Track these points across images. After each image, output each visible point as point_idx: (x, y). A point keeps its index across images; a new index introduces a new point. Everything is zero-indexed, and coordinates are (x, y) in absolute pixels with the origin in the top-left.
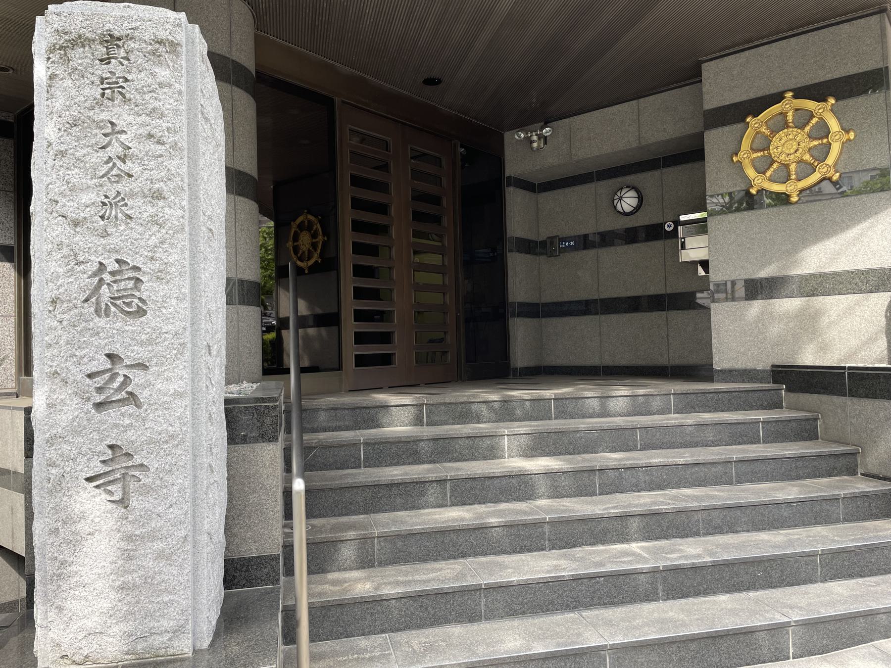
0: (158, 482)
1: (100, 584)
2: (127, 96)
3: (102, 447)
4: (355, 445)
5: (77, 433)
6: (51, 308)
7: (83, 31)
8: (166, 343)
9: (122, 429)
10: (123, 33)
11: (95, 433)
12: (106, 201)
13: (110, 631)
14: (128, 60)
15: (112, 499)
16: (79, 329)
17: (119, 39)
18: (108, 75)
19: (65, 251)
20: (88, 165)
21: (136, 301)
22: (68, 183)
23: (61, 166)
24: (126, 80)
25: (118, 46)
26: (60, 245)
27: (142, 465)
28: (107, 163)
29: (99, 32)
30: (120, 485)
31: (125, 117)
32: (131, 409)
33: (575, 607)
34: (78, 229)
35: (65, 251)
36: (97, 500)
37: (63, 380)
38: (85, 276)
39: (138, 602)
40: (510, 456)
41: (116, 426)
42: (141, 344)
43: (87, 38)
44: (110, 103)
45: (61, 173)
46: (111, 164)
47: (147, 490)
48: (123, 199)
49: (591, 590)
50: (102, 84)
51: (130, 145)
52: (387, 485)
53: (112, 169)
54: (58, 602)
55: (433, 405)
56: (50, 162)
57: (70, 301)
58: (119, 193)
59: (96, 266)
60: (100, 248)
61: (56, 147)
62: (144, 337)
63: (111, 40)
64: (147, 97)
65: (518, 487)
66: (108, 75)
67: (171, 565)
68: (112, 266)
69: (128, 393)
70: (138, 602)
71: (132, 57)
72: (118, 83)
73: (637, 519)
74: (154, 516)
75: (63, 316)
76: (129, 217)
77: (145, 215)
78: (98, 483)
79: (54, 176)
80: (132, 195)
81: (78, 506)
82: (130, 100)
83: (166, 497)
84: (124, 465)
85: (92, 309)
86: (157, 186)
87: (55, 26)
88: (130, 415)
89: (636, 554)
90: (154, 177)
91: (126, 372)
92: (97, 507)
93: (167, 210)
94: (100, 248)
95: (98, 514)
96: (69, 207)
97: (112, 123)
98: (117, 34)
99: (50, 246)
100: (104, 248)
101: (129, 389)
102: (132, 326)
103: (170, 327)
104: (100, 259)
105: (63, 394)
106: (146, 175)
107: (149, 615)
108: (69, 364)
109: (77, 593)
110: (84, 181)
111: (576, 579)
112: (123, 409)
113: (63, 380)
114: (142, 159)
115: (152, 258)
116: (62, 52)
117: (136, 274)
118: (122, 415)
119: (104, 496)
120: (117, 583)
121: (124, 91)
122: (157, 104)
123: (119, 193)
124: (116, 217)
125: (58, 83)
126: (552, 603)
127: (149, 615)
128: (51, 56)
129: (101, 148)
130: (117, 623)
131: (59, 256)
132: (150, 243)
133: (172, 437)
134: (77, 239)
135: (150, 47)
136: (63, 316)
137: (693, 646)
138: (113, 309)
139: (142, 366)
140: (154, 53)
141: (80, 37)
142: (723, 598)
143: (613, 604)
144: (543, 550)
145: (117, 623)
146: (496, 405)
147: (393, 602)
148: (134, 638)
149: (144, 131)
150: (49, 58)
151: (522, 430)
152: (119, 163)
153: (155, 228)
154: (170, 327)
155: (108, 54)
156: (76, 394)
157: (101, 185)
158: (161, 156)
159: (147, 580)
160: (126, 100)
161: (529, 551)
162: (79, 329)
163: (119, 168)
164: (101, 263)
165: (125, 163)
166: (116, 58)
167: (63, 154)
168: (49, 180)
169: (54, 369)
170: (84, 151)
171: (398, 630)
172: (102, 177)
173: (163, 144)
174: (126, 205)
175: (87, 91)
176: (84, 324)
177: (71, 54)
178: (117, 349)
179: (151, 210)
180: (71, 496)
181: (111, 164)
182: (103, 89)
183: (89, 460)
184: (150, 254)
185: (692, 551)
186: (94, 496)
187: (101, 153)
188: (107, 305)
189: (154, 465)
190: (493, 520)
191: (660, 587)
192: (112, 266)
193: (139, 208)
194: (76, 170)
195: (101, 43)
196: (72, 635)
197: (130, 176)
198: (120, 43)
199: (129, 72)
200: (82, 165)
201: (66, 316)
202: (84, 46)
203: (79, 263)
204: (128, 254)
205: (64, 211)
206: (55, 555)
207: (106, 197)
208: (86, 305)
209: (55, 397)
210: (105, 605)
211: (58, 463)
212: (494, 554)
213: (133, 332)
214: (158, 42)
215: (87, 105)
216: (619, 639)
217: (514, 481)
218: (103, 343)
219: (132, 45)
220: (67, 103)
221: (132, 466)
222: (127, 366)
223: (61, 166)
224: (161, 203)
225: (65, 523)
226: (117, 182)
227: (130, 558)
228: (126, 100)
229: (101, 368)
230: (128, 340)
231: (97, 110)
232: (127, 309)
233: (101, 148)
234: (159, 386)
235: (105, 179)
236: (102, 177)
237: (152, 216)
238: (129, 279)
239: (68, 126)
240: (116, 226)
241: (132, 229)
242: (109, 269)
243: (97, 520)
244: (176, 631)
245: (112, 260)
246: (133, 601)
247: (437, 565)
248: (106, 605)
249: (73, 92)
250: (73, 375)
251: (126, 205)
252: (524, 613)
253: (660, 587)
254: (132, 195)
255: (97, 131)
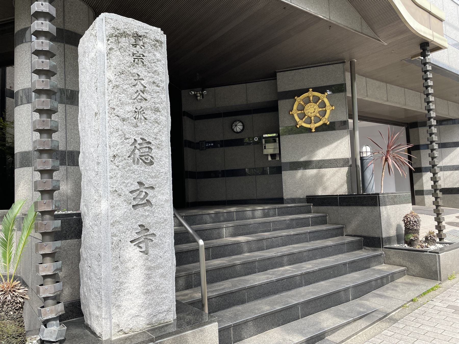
0: (160, 241)
1: (137, 292)
2: (145, 63)
3: (136, 226)
4: (279, 215)
5: (126, 220)
6: (112, 160)
7: (125, 30)
8: (162, 177)
9: (145, 217)
10: (143, 34)
11: (133, 220)
12: (136, 110)
13: (142, 314)
14: (144, 47)
15: (142, 250)
16: (126, 170)
17: (140, 36)
18: (136, 52)
19: (120, 132)
20: (128, 93)
21: (150, 158)
22: (120, 100)
23: (116, 92)
24: (143, 56)
25: (140, 40)
26: (117, 130)
27: (154, 234)
28: (136, 93)
29: (132, 32)
30: (144, 244)
31: (144, 73)
32: (147, 208)
33: (277, 293)
34: (124, 123)
35: (120, 132)
36: (136, 251)
37: (118, 194)
38: (129, 145)
39: (153, 299)
40: (226, 237)
41: (142, 216)
42: (152, 177)
43: (127, 34)
44: (137, 66)
45: (116, 95)
46: (138, 94)
47: (156, 245)
48: (143, 110)
49: (282, 285)
50: (133, 56)
51: (146, 86)
52: (185, 252)
53: (138, 96)
54: (118, 303)
55: (187, 216)
56: (110, 89)
57: (123, 157)
58: (142, 107)
59: (133, 141)
60: (134, 132)
61: (114, 83)
62: (153, 174)
63: (137, 37)
64: (153, 65)
65: (235, 249)
66: (136, 52)
67: (165, 280)
68: (141, 141)
69: (147, 200)
70: (153, 299)
71: (146, 46)
72: (140, 57)
73: (286, 257)
74: (159, 257)
75: (119, 164)
76: (146, 119)
77: (152, 118)
78: (136, 243)
79: (113, 97)
80: (147, 109)
81: (127, 254)
82: (145, 65)
83: (163, 248)
84: (146, 234)
85: (132, 161)
86: (157, 106)
87: (112, 25)
88: (148, 211)
89: (288, 271)
90: (156, 101)
91: (146, 190)
92: (136, 255)
93: (161, 117)
94: (134, 132)
95: (136, 258)
96: (121, 112)
97: (138, 75)
98: (140, 34)
99: (112, 130)
100: (136, 133)
101: (147, 198)
102: (148, 169)
103: (164, 170)
104: (134, 137)
105: (119, 201)
106: (153, 100)
107: (158, 304)
108: (122, 186)
109: (127, 297)
110: (127, 100)
111: (278, 281)
112: (146, 208)
113: (118, 194)
114: (151, 93)
115: (155, 139)
116: (116, 38)
117: (149, 145)
118: (145, 210)
119: (138, 249)
120: (145, 291)
121: (143, 61)
122: (156, 69)
123: (142, 107)
124: (141, 119)
125: (113, 52)
126: (269, 292)
127: (158, 304)
128: (110, 39)
129: (134, 86)
130: (145, 310)
131: (117, 135)
132: (155, 131)
133: (165, 220)
134: (125, 127)
135: (153, 43)
136: (119, 164)
137: (324, 299)
138: (141, 161)
139: (152, 188)
140: (155, 45)
141: (124, 32)
142: (322, 283)
143: (289, 290)
144: (256, 273)
145: (145, 310)
146: (213, 215)
147: (213, 299)
148: (152, 316)
149: (151, 80)
150: (108, 40)
151: (230, 225)
152: (141, 94)
153: (156, 125)
154: (164, 170)
155: (135, 42)
156: (125, 201)
157: (134, 103)
158: (158, 92)
159: (157, 288)
160: (144, 65)
161: (251, 274)
162: (126, 170)
163: (141, 96)
164: (135, 140)
165: (144, 93)
166: (139, 45)
167: (117, 86)
168: (110, 98)
169: (114, 189)
170: (127, 86)
171: (215, 312)
172: (134, 99)
173: (159, 87)
174: (144, 113)
175: (127, 58)
176: (128, 168)
177: (120, 40)
178: (143, 181)
179: (155, 116)
180: (124, 250)
181: (138, 94)
182: (134, 59)
183: (131, 232)
184: (155, 136)
185: (309, 266)
186: (134, 250)
187: (133, 88)
188: (138, 159)
189: (158, 234)
190: (238, 262)
191: (303, 281)
192: (140, 141)
193: (149, 114)
194: (123, 95)
195: (133, 37)
196: (125, 319)
197: (146, 100)
198: (141, 38)
199: (144, 52)
200: (126, 93)
201: (121, 164)
202: (125, 37)
203: (126, 139)
204: (146, 136)
205: (118, 113)
206: (117, 279)
207: (136, 109)
208: (129, 158)
209: (115, 203)
210: (140, 302)
211: (117, 234)
212: (238, 277)
213: (149, 172)
214: (156, 41)
215: (128, 65)
216: (302, 300)
217: (235, 246)
218: (137, 176)
219: (146, 40)
220: (119, 63)
221: (149, 235)
222: (147, 188)
223: (116, 92)
224: (158, 114)
225: (122, 263)
226: (140, 102)
227: (149, 278)
228: (144, 65)
229: (136, 188)
230: (146, 176)
231: (132, 68)
232: (146, 161)
233: (134, 86)
234: (159, 197)
235: (136, 100)
236: (134, 99)
237: (155, 119)
238: (146, 147)
239: (119, 73)
240: (141, 122)
241: (147, 124)
242: (139, 142)
243: (136, 261)
244: (168, 311)
245: (139, 138)
246: (151, 298)
247: (221, 283)
248: (140, 301)
249: (121, 58)
250: (124, 192)
251: (144, 113)
252: (260, 298)
253: (303, 281)
254: (147, 109)
255: (132, 78)
